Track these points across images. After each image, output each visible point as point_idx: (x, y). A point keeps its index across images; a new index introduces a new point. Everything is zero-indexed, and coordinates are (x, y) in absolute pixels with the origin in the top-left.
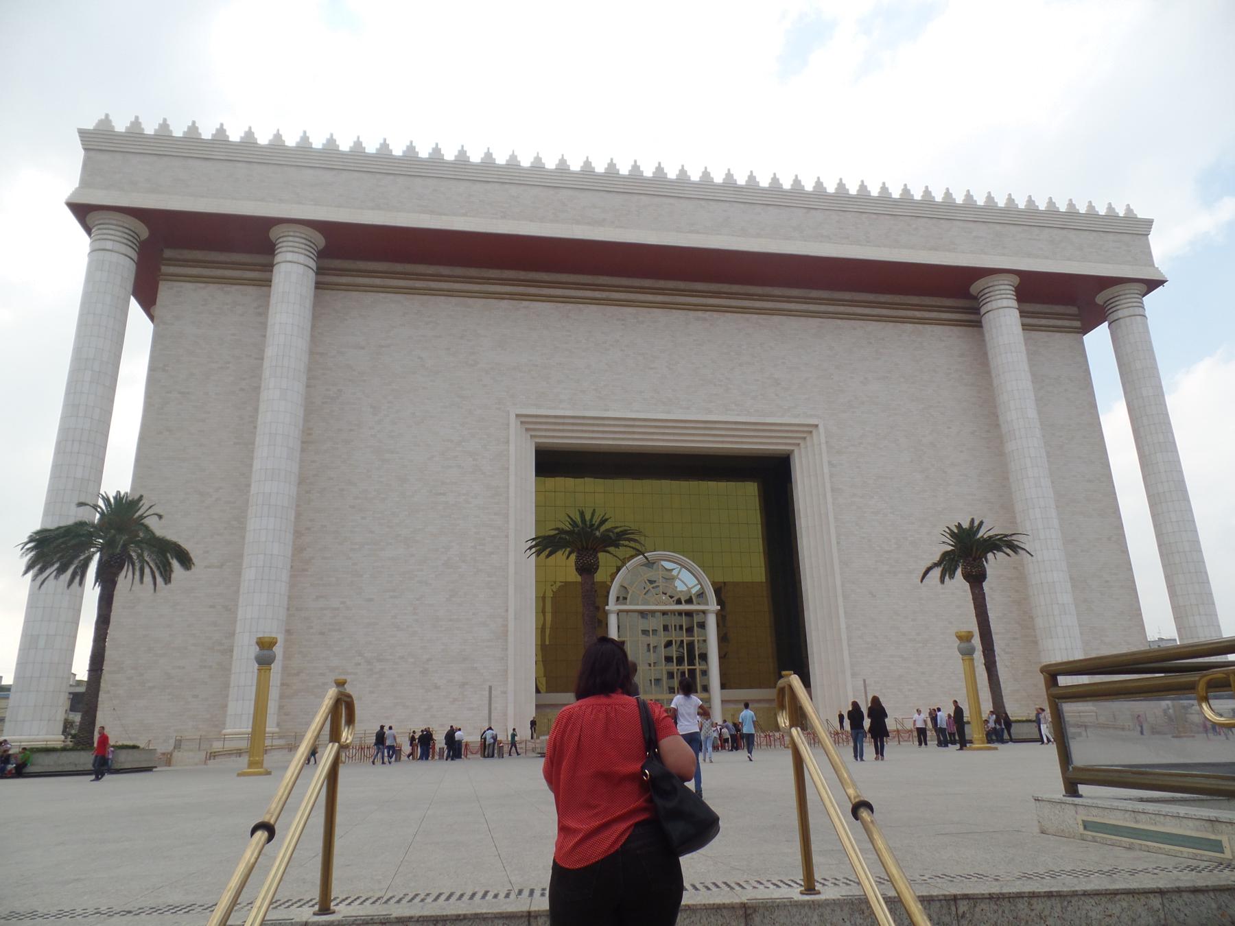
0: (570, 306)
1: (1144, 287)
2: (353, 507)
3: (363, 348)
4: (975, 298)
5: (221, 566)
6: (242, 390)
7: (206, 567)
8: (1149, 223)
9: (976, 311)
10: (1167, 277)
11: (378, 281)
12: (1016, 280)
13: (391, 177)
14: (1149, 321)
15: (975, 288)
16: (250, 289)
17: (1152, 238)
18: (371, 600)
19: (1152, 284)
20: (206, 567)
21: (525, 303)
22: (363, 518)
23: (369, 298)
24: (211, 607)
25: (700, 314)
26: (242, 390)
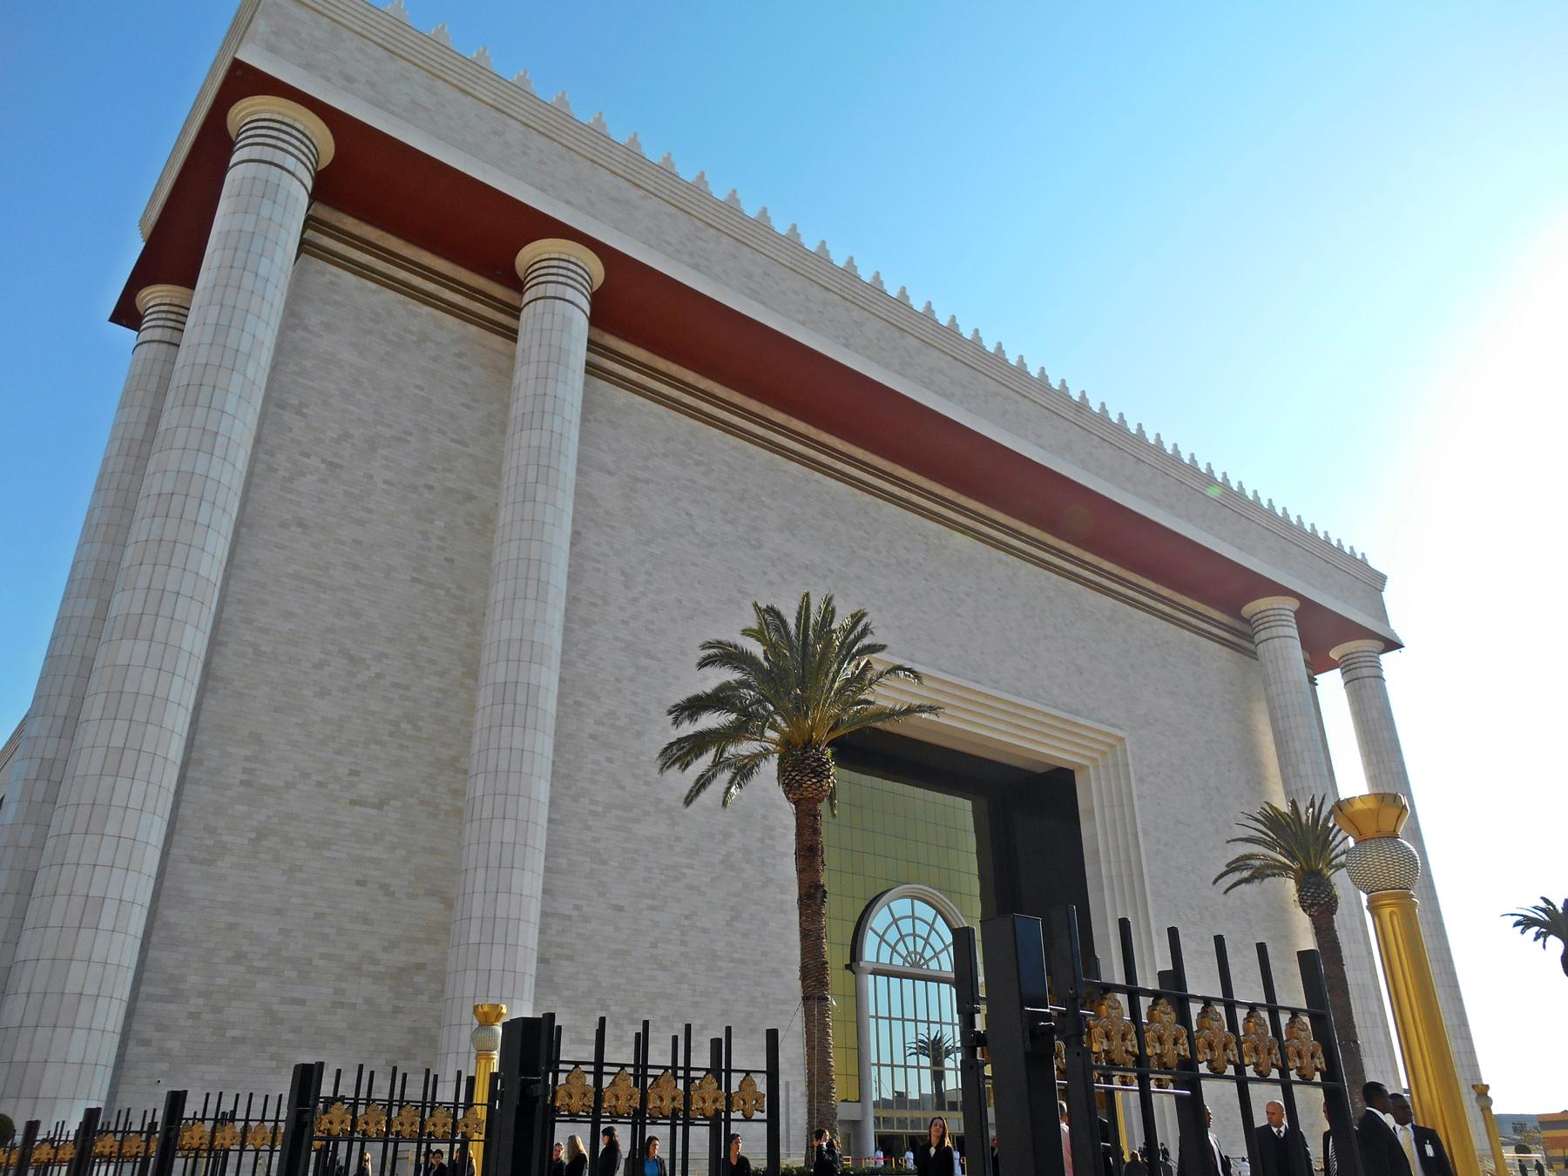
0: (868, 498)
1: (1380, 645)
2: (593, 737)
3: (609, 473)
4: (1247, 621)
5: (380, 806)
6: (430, 488)
7: (353, 803)
8: (1382, 579)
9: (1250, 638)
10: (1404, 641)
11: (633, 375)
12: (1294, 604)
13: (712, 231)
14: (1387, 684)
15: (1249, 609)
16: (449, 320)
17: (1389, 596)
18: (619, 908)
19: (1393, 645)
20: (353, 803)
21: (818, 475)
22: (610, 760)
23: (622, 396)
24: (360, 883)
25: (1002, 554)
26: (430, 488)
